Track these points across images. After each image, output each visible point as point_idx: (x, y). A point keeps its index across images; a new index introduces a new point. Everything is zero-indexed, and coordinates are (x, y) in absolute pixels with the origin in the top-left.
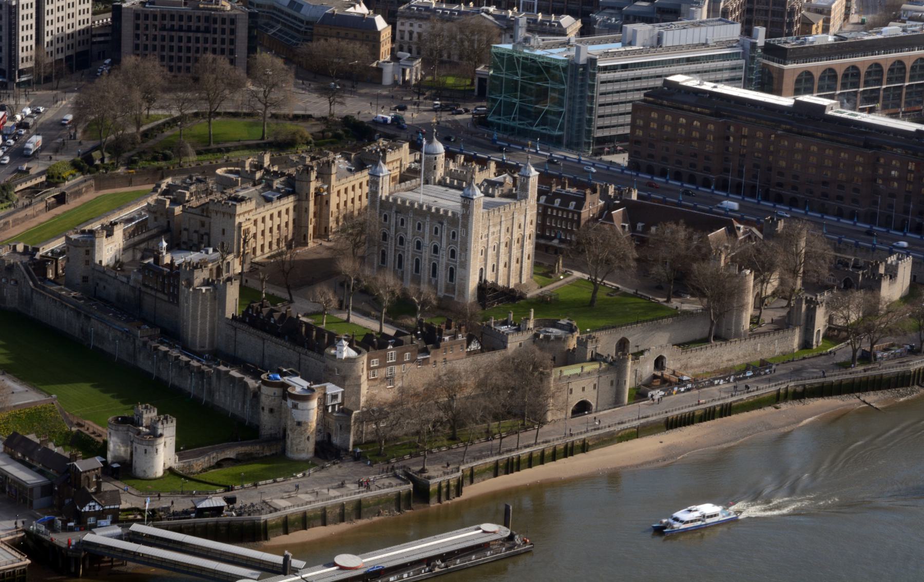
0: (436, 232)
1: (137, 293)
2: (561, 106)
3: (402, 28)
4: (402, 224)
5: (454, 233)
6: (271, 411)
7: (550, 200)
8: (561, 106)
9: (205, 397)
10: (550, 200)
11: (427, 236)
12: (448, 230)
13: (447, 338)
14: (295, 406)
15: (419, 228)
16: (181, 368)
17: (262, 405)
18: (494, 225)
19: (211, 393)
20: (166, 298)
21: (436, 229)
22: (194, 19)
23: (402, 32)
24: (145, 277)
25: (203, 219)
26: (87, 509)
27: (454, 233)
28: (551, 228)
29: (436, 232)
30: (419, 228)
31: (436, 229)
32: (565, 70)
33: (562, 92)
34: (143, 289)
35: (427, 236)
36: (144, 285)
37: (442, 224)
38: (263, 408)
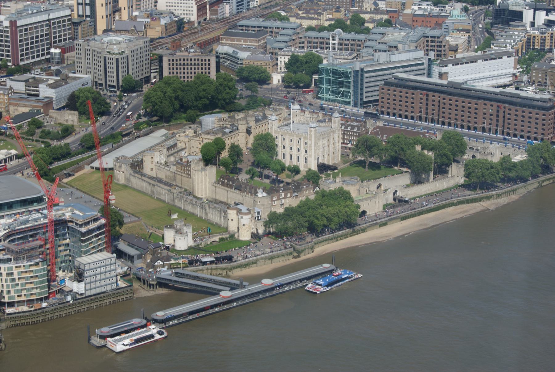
2: (350, 88)
3: (281, 60)
7: (346, 127)
8: (350, 88)
9: (204, 216)
10: (346, 127)
13: (305, 187)
14: (242, 217)
18: (323, 139)
19: (206, 214)
20: (186, 175)
22: (193, 60)
23: (281, 61)
24: (177, 167)
26: (157, 264)
28: (347, 139)
32: (350, 73)
34: (176, 172)
37: (300, 139)
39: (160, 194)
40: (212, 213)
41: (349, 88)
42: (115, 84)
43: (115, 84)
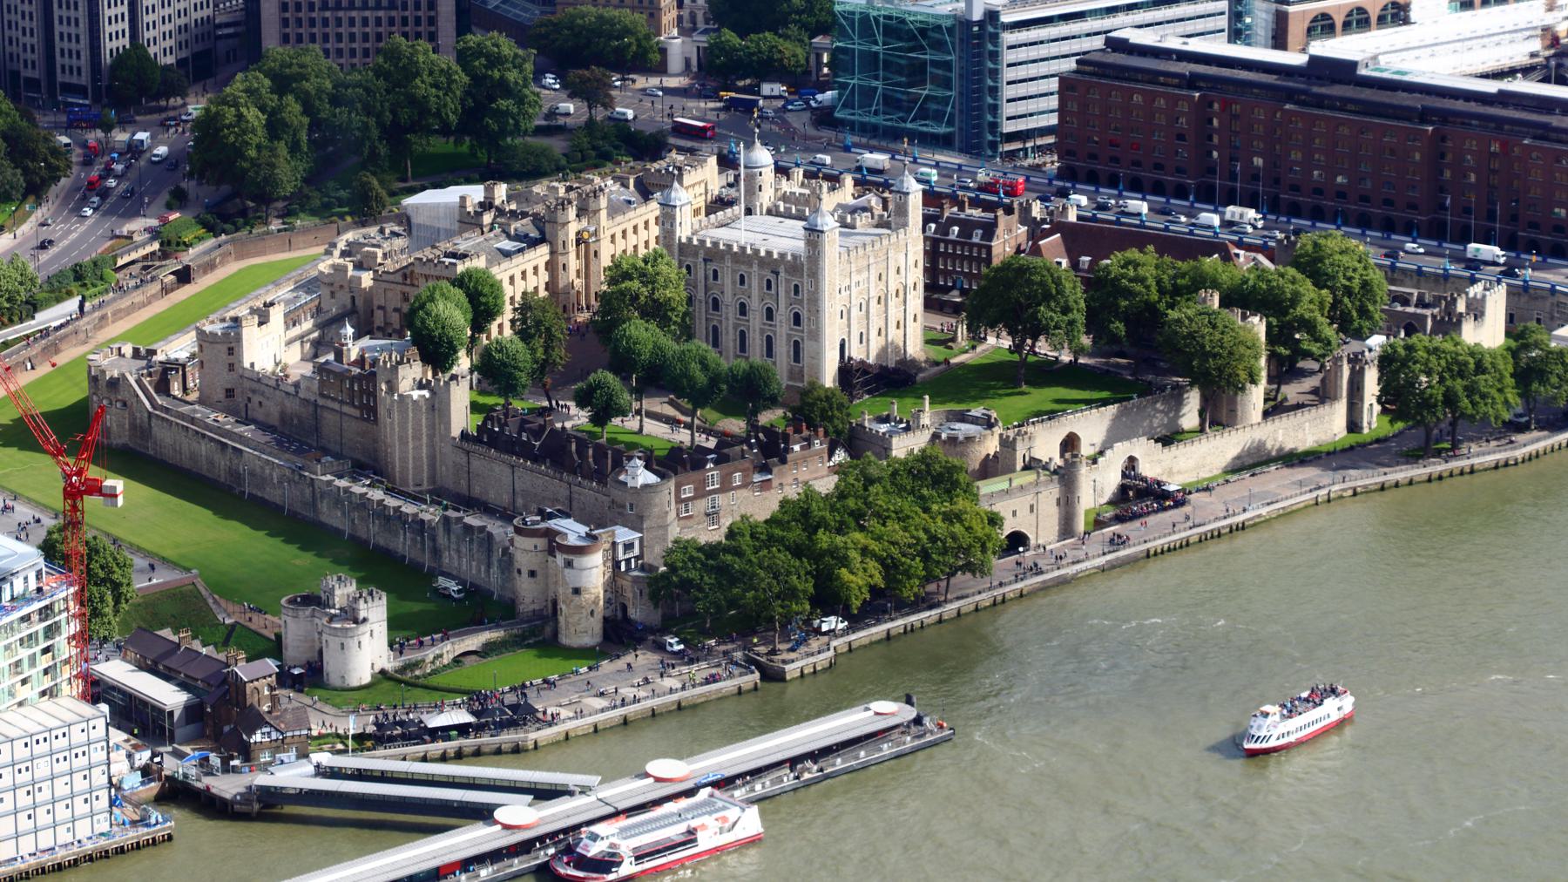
0: (769, 287)
1: (311, 409)
4: (715, 277)
5: (796, 287)
6: (532, 574)
7: (944, 229)
10: (944, 229)
11: (755, 292)
12: (787, 281)
13: (797, 448)
14: (569, 564)
15: (742, 282)
16: (388, 519)
17: (517, 565)
18: (859, 271)
19: (436, 552)
20: (357, 413)
21: (769, 282)
25: (407, 289)
27: (796, 287)
28: (946, 273)
29: (769, 287)
30: (742, 282)
31: (769, 282)
32: (950, 30)
33: (947, 66)
34: (321, 402)
35: (755, 292)
36: (322, 395)
37: (777, 274)
38: (519, 571)
39: (263, 481)
40: (458, 551)
41: (947, 84)
42: (85, 79)
43: (85, 79)
